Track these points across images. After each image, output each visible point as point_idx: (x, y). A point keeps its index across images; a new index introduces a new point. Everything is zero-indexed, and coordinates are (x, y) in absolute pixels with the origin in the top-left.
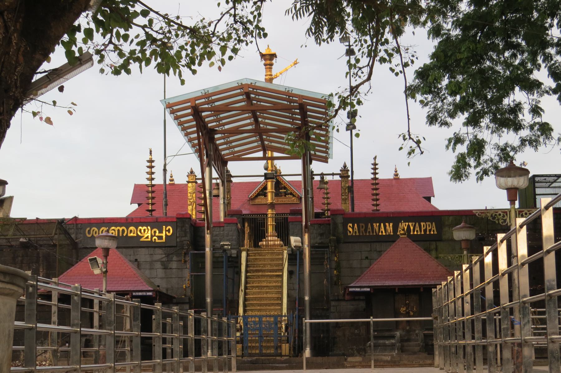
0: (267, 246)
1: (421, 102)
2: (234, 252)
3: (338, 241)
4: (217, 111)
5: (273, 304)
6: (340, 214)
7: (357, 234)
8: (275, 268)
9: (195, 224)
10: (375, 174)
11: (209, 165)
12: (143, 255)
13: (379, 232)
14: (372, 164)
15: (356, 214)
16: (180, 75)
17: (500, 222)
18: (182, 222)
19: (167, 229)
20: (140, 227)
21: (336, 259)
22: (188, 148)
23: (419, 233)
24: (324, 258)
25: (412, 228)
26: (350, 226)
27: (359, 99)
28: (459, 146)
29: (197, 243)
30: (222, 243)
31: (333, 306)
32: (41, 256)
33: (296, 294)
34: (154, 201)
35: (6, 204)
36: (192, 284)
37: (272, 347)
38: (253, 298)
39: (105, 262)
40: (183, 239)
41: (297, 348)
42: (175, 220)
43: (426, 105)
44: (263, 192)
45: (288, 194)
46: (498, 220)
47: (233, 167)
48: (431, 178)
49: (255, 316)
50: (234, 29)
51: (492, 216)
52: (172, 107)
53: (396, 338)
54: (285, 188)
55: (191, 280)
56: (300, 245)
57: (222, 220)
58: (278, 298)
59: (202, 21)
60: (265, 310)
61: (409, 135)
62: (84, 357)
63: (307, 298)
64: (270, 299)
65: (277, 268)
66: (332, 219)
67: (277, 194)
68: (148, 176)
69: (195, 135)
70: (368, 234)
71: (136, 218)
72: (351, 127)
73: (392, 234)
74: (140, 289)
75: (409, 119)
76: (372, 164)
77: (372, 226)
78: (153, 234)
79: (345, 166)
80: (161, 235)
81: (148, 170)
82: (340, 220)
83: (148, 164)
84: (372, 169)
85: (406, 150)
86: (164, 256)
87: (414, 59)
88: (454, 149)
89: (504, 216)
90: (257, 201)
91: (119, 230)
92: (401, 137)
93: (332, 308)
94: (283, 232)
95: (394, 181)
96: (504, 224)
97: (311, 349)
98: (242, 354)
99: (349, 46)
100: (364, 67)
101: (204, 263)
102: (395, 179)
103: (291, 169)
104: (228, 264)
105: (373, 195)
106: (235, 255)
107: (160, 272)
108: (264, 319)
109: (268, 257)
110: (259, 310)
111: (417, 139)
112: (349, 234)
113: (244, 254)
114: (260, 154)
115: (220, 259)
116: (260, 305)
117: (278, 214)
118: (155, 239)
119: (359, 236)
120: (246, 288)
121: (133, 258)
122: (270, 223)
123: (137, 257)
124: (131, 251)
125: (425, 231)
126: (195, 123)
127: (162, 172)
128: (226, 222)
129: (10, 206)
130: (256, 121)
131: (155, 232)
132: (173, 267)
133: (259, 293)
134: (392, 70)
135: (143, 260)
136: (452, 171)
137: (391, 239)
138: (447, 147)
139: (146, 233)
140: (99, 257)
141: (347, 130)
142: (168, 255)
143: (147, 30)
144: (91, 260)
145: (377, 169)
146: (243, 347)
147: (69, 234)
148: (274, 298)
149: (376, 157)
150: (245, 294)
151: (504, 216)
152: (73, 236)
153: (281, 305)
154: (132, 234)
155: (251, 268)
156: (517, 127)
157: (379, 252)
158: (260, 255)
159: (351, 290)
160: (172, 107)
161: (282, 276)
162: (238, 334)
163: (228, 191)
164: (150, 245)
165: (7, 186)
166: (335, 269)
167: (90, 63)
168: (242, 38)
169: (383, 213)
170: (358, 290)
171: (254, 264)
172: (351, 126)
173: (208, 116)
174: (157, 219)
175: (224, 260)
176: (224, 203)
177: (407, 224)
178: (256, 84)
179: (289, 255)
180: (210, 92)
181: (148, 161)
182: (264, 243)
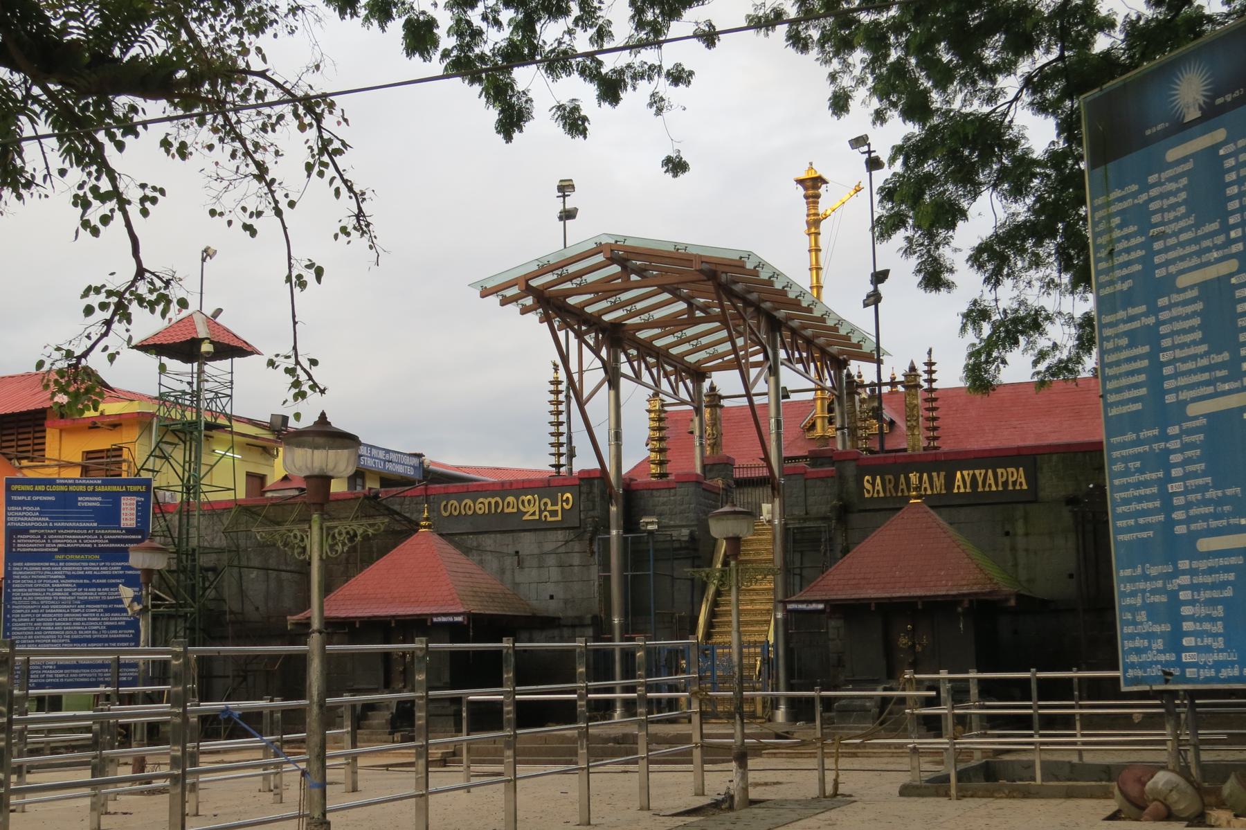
7: (882, 495)
12: (528, 544)
23: (962, 490)
24: (819, 540)
25: (980, 480)
40: (591, 513)
42: (577, 482)
71: (517, 481)
75: (295, 323)
77: (908, 480)
79: (913, 368)
80: (555, 508)
82: (850, 470)
83: (552, 387)
91: (490, 503)
93: (831, 631)
96: (302, 557)
99: (869, 152)
107: (554, 573)
119: (885, 497)
121: (511, 550)
124: (508, 538)
125: (1005, 483)
131: (546, 504)
137: (892, 505)
139: (531, 507)
154: (510, 510)
164: (539, 527)
181: (552, 383)
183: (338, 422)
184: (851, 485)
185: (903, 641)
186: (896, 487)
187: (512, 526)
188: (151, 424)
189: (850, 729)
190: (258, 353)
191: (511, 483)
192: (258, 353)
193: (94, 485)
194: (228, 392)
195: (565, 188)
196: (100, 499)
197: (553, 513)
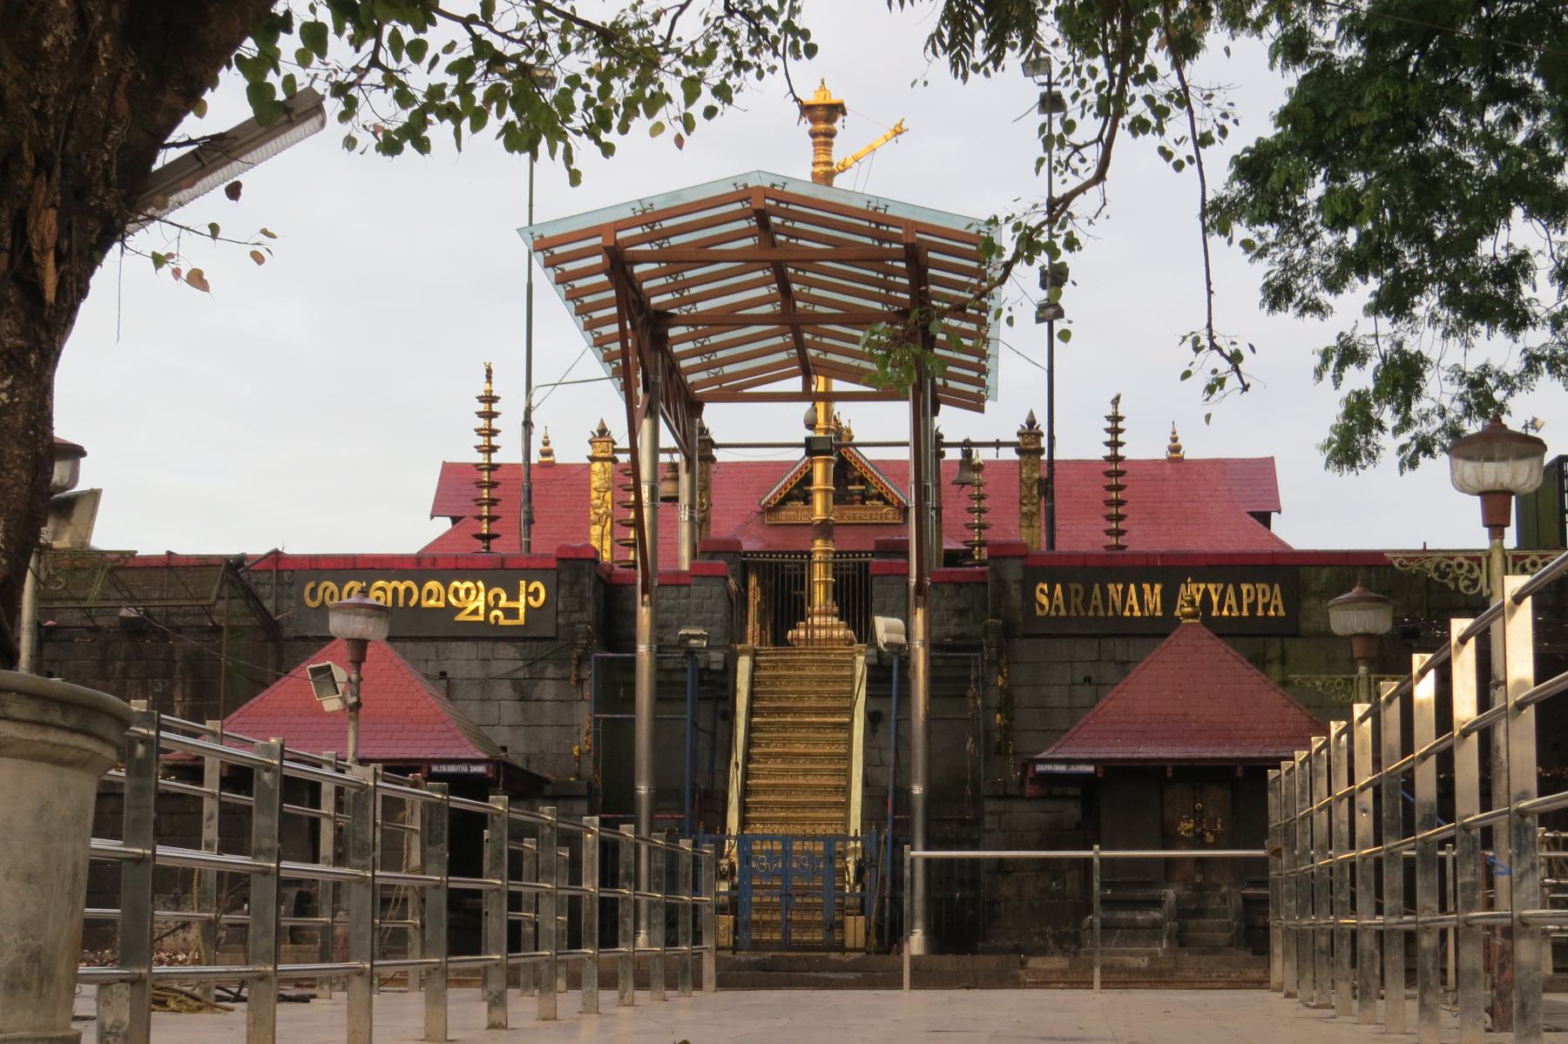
0: (810, 641)
1: (1247, 245)
2: (717, 656)
3: (1008, 632)
4: (676, 261)
6: (1014, 557)
7: (1063, 613)
8: (830, 703)
9: (610, 575)
10: (1115, 444)
11: (651, 412)
12: (463, 661)
13: (1123, 609)
14: (1108, 418)
15: (1060, 556)
16: (568, 158)
17: (1462, 586)
18: (574, 570)
19: (531, 589)
20: (456, 584)
21: (1000, 681)
22: (593, 365)
23: (1235, 614)
24: (967, 679)
26: (1042, 591)
27: (1070, 234)
28: (1351, 371)
29: (614, 628)
30: (683, 632)
31: (992, 813)
32: (177, 657)
33: (886, 778)
34: (495, 511)
35: (79, 512)
36: (596, 746)
37: (819, 924)
38: (767, 786)
39: (354, 677)
40: (576, 617)
41: (887, 927)
43: (1262, 253)
44: (801, 490)
45: (871, 498)
46: (1456, 579)
47: (719, 419)
48: (1272, 459)
49: (772, 838)
50: (726, 31)
51: (1437, 568)
52: (550, 249)
53: (1166, 907)
54: (862, 480)
55: (596, 733)
56: (903, 639)
57: (685, 566)
58: (837, 787)
59: (634, 8)
60: (801, 821)
61: (1211, 337)
62: (293, 942)
63: (917, 790)
64: (814, 789)
65: (836, 704)
66: (994, 569)
67: (840, 497)
68: (481, 441)
70: (1091, 613)
71: (445, 557)
72: (1049, 312)
73: (1159, 614)
74: (453, 756)
75: (1210, 293)
76: (1108, 418)
78: (492, 603)
79: (1031, 422)
80: (513, 605)
81: (482, 423)
82: (1013, 572)
83: (482, 407)
84: (1108, 430)
85: (1202, 379)
86: (521, 663)
87: (1228, 124)
88: (1337, 380)
89: (1471, 570)
90: (785, 515)
91: (395, 590)
92: (1189, 344)
93: (987, 818)
94: (855, 602)
95: (1168, 466)
96: (1472, 592)
97: (927, 933)
98: (735, 942)
99: (1049, 84)
100: (1086, 145)
101: (631, 686)
102: (1170, 460)
103: (879, 427)
104: (700, 689)
105: (1109, 503)
106: (719, 667)
107: (509, 710)
108: (797, 846)
111: (1233, 348)
112: (1039, 612)
113: (744, 664)
115: (678, 677)
117: (841, 553)
118: (497, 618)
119: (1067, 617)
120: (748, 758)
121: (433, 669)
122: (820, 576)
123: (446, 667)
124: (428, 650)
125: (1253, 607)
126: (612, 293)
127: (520, 429)
128: (696, 574)
129: (92, 516)
130: (785, 290)
131: (497, 597)
132: (547, 697)
134: (1165, 154)
135: (461, 674)
136: (1330, 442)
137: (1159, 629)
138: (1319, 373)
139: (473, 600)
140: (339, 663)
141: (1039, 320)
142: (531, 663)
143: (477, 29)
144: (315, 672)
145: (1121, 431)
146: (736, 923)
147: (257, 599)
148: (826, 786)
149: (1118, 398)
150: (746, 775)
151: (1471, 570)
152: (269, 604)
153: (846, 806)
154: (432, 603)
155: (764, 704)
156: (1517, 320)
157: (1123, 663)
158: (789, 668)
159: (1040, 768)
160: (550, 249)
161: (848, 727)
162: (724, 887)
163: (702, 487)
164: (483, 634)
165: (82, 460)
166: (999, 710)
167: (314, 121)
168: (746, 57)
169: (1135, 555)
170: (1061, 768)
171: (773, 692)
172: (1051, 311)
173: (651, 276)
174: (503, 559)
175: (689, 677)
176: (691, 518)
177: (1202, 586)
178: (788, 189)
179: (870, 667)
180: (656, 208)
181: (482, 399)
182: (802, 633)
184: (1015, 592)
186: (1086, 602)
197: (511, 613)
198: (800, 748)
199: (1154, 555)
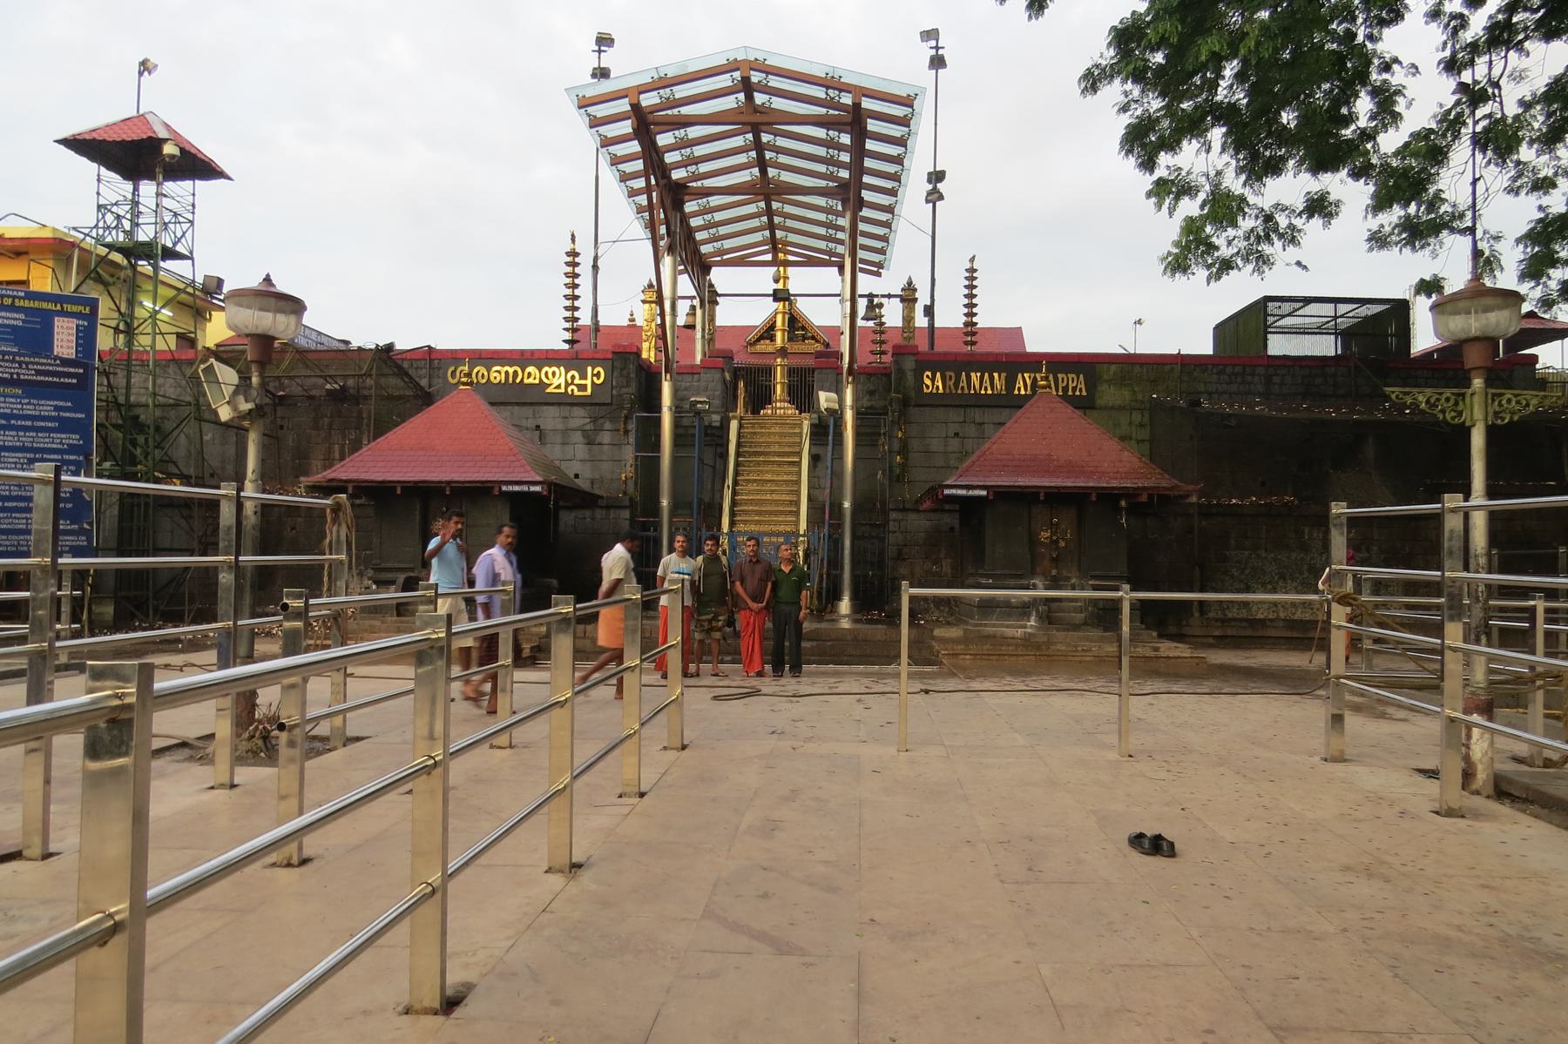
2: (716, 418)
3: (905, 403)
5: (782, 513)
11: (671, 249)
12: (550, 418)
22: (638, 230)
29: (651, 400)
33: (825, 496)
40: (624, 390)
44: (768, 332)
54: (803, 328)
57: (698, 358)
60: (769, 523)
63: (847, 505)
66: (896, 362)
68: (569, 280)
69: (640, 183)
77: (969, 378)
82: (909, 364)
90: (760, 348)
94: (802, 396)
97: (851, 599)
99: (937, 48)
101: (658, 436)
104: (701, 438)
107: (581, 450)
109: (777, 430)
110: (758, 522)
113: (734, 425)
114: (768, 257)
115: (690, 431)
116: (760, 513)
120: (736, 483)
121: (531, 423)
123: (540, 422)
124: (528, 411)
125: (1065, 389)
128: (705, 366)
131: (573, 377)
133: (758, 492)
136: (1169, 254)
139: (557, 379)
141: (927, 201)
142: (594, 420)
150: (734, 493)
152: (424, 382)
153: (797, 513)
154: (531, 381)
159: (947, 492)
161: (799, 464)
164: (564, 401)
179: (812, 426)
181: (568, 254)
183: (282, 286)
184: (910, 376)
185: (1045, 535)
187: (536, 398)
188: (69, 259)
189: (994, 626)
190: (229, 178)
191: (533, 352)
192: (229, 178)
193: (14, 297)
194: (190, 216)
195: (604, 41)
196: (22, 316)
197: (582, 388)
198: (769, 477)
199: (1001, 355)
